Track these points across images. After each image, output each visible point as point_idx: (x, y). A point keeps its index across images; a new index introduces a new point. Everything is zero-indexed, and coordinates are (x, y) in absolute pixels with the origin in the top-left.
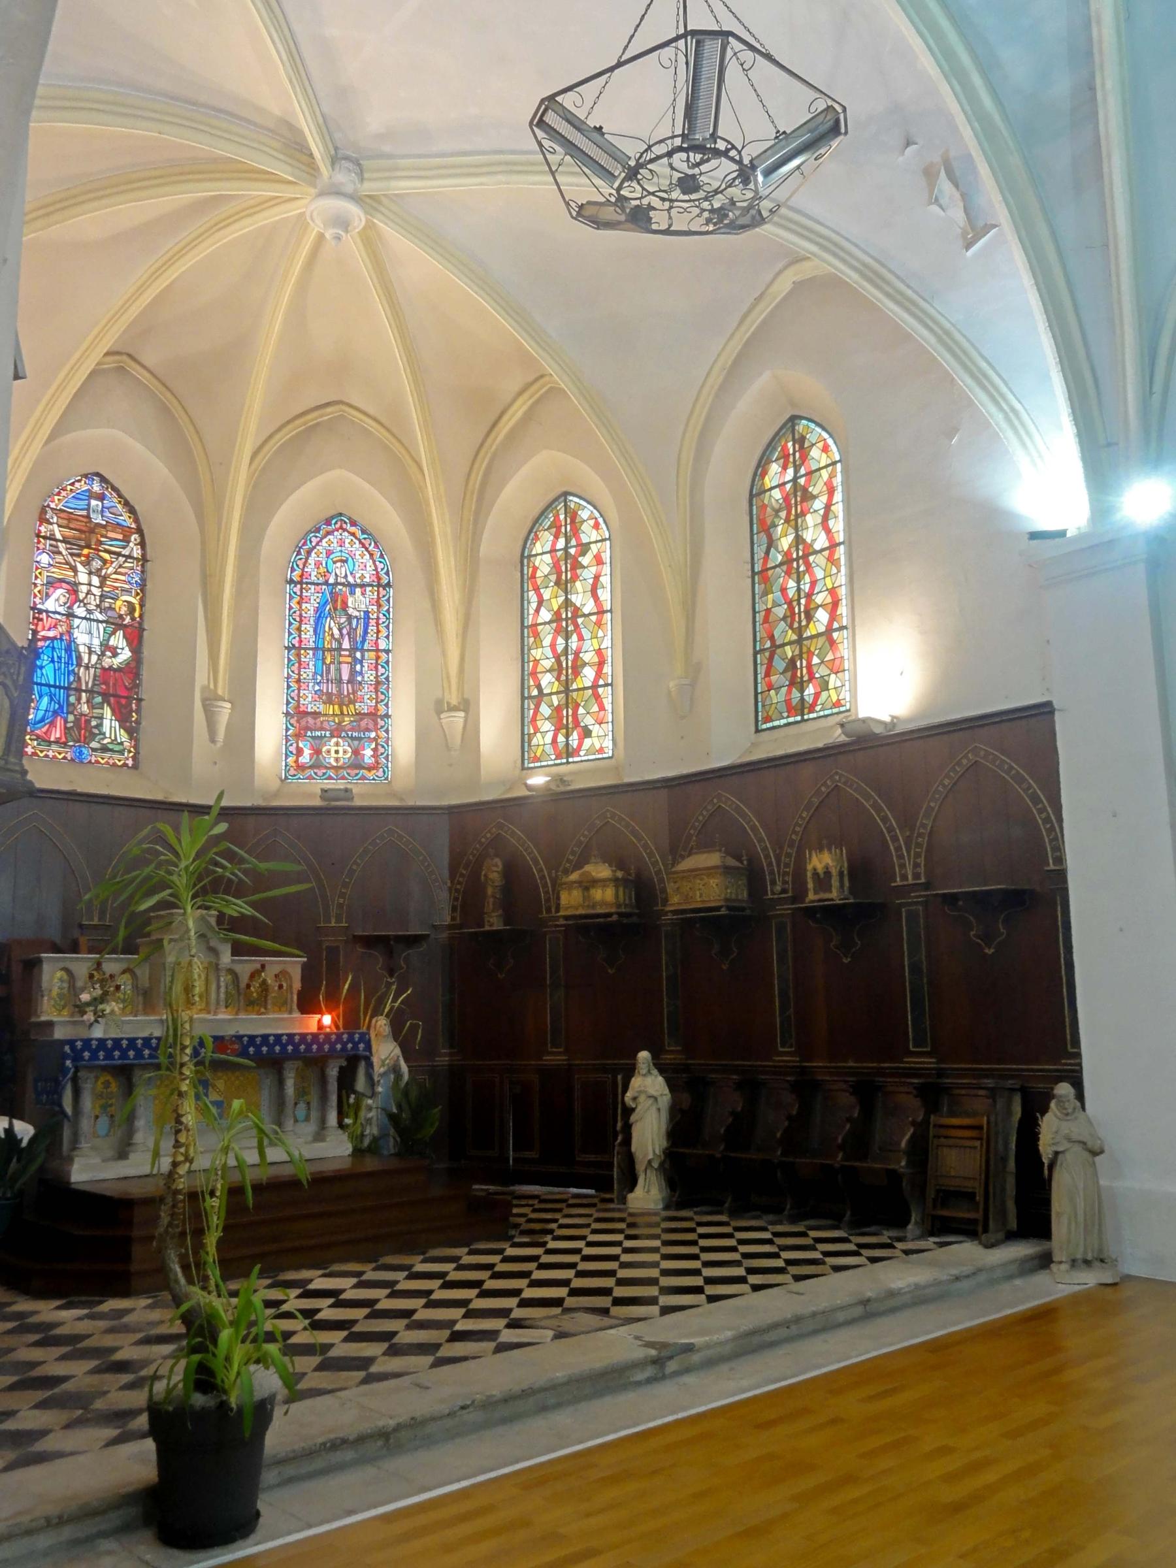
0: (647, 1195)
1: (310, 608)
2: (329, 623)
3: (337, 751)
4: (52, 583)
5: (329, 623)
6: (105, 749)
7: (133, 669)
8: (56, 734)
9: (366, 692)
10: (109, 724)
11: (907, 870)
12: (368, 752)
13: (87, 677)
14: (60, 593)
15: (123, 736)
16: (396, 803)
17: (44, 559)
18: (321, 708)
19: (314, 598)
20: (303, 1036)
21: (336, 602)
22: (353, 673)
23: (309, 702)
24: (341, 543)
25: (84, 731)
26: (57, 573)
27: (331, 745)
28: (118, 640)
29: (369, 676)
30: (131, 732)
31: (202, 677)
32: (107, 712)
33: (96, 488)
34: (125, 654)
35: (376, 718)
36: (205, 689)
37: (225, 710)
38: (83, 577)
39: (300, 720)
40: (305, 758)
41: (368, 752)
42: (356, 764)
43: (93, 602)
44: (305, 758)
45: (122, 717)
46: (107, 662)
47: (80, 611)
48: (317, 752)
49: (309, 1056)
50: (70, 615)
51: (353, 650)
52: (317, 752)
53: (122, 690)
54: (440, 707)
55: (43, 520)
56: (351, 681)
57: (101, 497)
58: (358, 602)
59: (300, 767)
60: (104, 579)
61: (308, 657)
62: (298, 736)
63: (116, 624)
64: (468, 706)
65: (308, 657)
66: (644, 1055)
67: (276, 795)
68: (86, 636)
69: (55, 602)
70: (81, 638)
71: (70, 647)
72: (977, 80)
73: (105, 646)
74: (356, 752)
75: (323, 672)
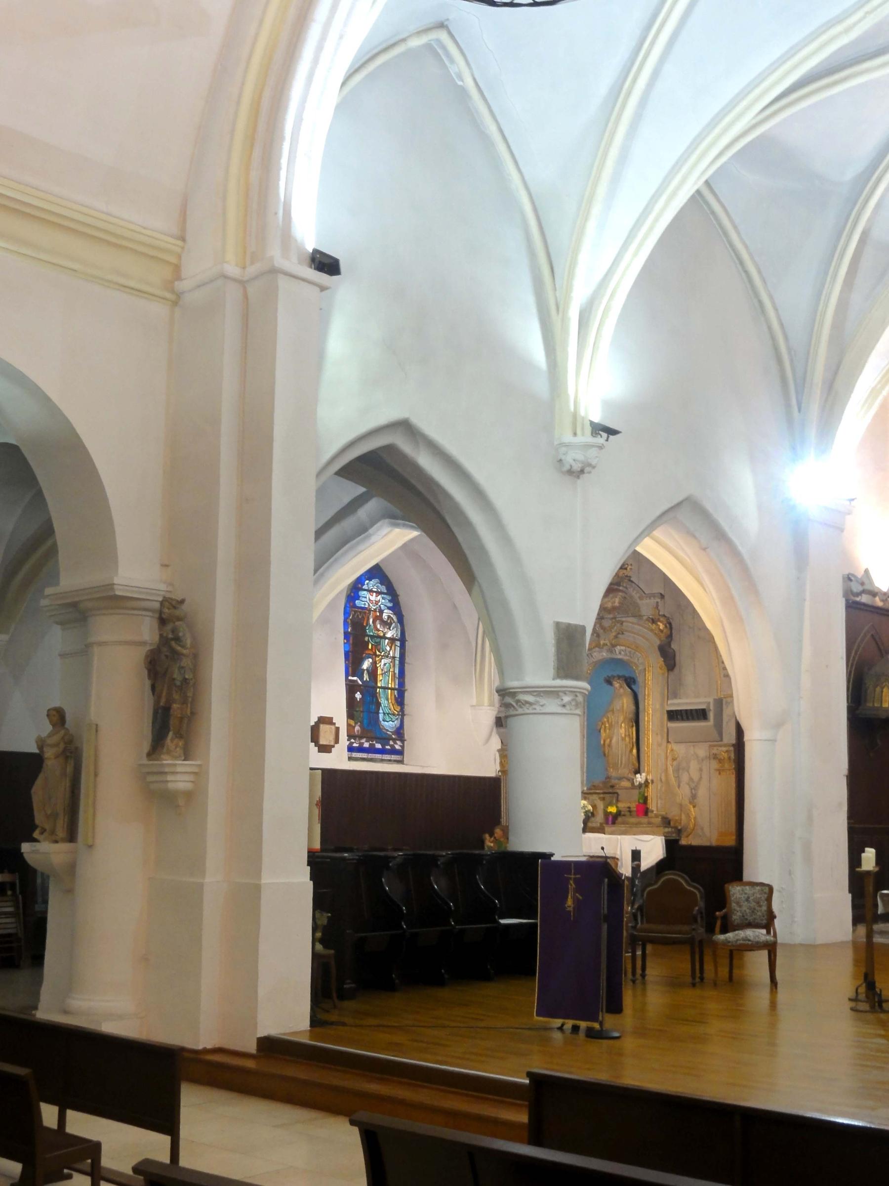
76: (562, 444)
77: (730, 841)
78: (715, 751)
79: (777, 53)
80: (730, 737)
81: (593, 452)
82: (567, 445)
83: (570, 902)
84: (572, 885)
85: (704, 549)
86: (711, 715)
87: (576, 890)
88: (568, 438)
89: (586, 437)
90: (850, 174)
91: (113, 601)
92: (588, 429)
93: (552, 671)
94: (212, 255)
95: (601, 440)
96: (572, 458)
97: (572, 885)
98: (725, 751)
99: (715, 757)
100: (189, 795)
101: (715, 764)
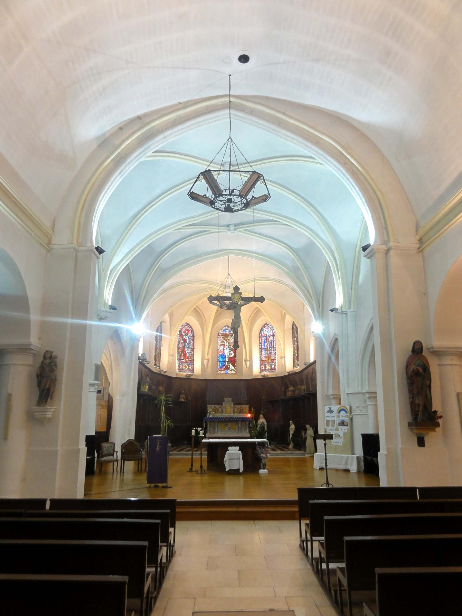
0: (291, 446)
1: (263, 341)
2: (266, 343)
3: (268, 367)
4: (221, 345)
5: (266, 343)
6: (231, 371)
7: (234, 357)
8: (223, 369)
9: (272, 355)
10: (231, 366)
11: (311, 389)
12: (273, 367)
13: (227, 359)
14: (222, 346)
15: (233, 368)
16: (275, 376)
17: (219, 342)
18: (265, 359)
19: (263, 339)
20: (246, 417)
21: (267, 340)
22: (270, 352)
23: (264, 359)
24: (267, 328)
25: (227, 368)
26: (221, 343)
27: (267, 366)
28: (232, 352)
29: (273, 352)
30: (234, 367)
31: (244, 357)
32: (231, 364)
33: (227, 328)
34: (233, 354)
35: (274, 360)
36: (245, 359)
37: (248, 362)
38: (225, 342)
39: (262, 362)
40: (263, 369)
41: (273, 367)
42: (271, 369)
43: (227, 347)
44: (263, 369)
45: (233, 365)
46: (230, 356)
47: (225, 349)
48: (265, 367)
49: (244, 420)
50: (224, 350)
51: (270, 348)
52: (265, 367)
53: (232, 361)
54: (282, 358)
55: (219, 335)
56: (270, 354)
57: (228, 329)
58: (270, 339)
59: (263, 370)
60: (229, 343)
61: (263, 350)
62: (262, 365)
63: (231, 350)
64: (284, 358)
65: (263, 350)
66: (291, 421)
67: (258, 376)
68: (227, 353)
69: (221, 348)
70: (226, 353)
71: (224, 355)
72: (283, 267)
73: (230, 354)
74: (271, 367)
75: (265, 353)
76: (100, 310)
77: (104, 430)
78: (101, 403)
79: (176, 220)
80: (106, 398)
81: (109, 314)
82: (103, 311)
83: (158, 449)
84: (158, 444)
85: (115, 344)
86: (102, 392)
87: (160, 445)
88: (102, 308)
89: (108, 310)
90: (160, 250)
91: (25, 349)
92: (108, 307)
93: (93, 378)
94: (62, 239)
95: (112, 311)
96: (103, 314)
97: (158, 444)
98: (104, 403)
99: (101, 405)
100: (49, 420)
101: (100, 407)
